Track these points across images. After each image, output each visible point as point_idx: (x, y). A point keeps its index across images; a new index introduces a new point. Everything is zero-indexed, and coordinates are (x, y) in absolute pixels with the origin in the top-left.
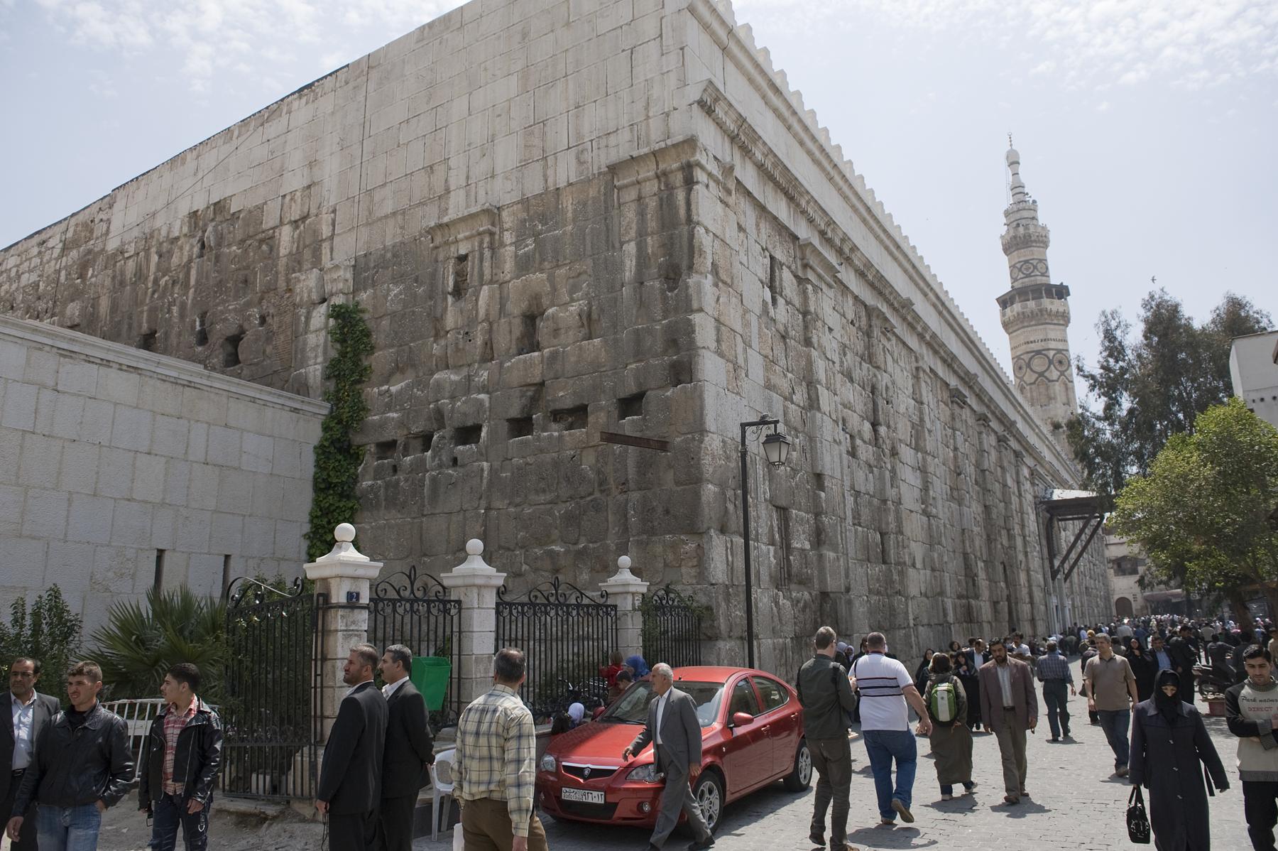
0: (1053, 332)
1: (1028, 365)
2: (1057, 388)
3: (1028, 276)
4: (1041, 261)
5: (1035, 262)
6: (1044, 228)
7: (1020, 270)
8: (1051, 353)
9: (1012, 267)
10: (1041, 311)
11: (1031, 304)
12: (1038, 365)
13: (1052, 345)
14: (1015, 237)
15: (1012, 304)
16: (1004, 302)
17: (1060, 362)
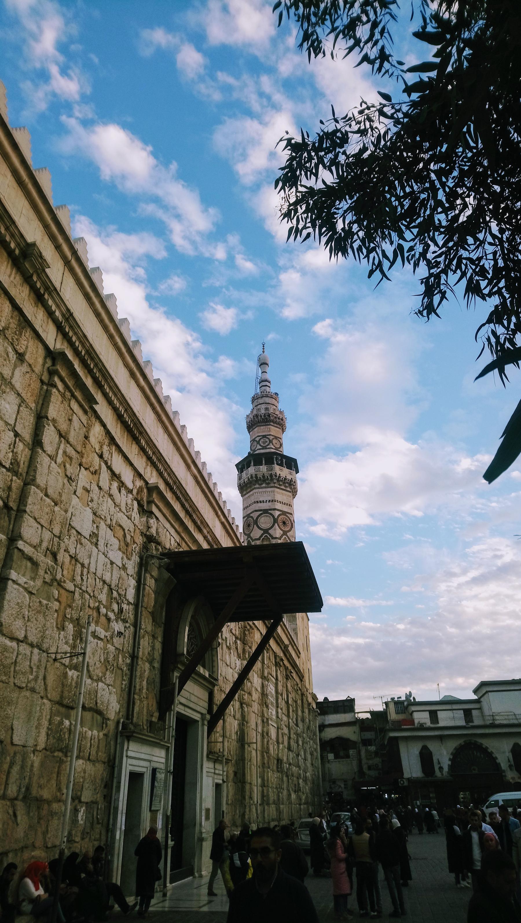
0: (280, 495)
1: (256, 522)
3: (264, 448)
4: (276, 438)
5: (271, 438)
6: (281, 412)
7: (258, 442)
8: (277, 513)
9: (253, 441)
11: (264, 468)
12: (265, 522)
13: (278, 506)
14: (257, 416)
15: (249, 466)
16: (241, 467)
17: (284, 523)
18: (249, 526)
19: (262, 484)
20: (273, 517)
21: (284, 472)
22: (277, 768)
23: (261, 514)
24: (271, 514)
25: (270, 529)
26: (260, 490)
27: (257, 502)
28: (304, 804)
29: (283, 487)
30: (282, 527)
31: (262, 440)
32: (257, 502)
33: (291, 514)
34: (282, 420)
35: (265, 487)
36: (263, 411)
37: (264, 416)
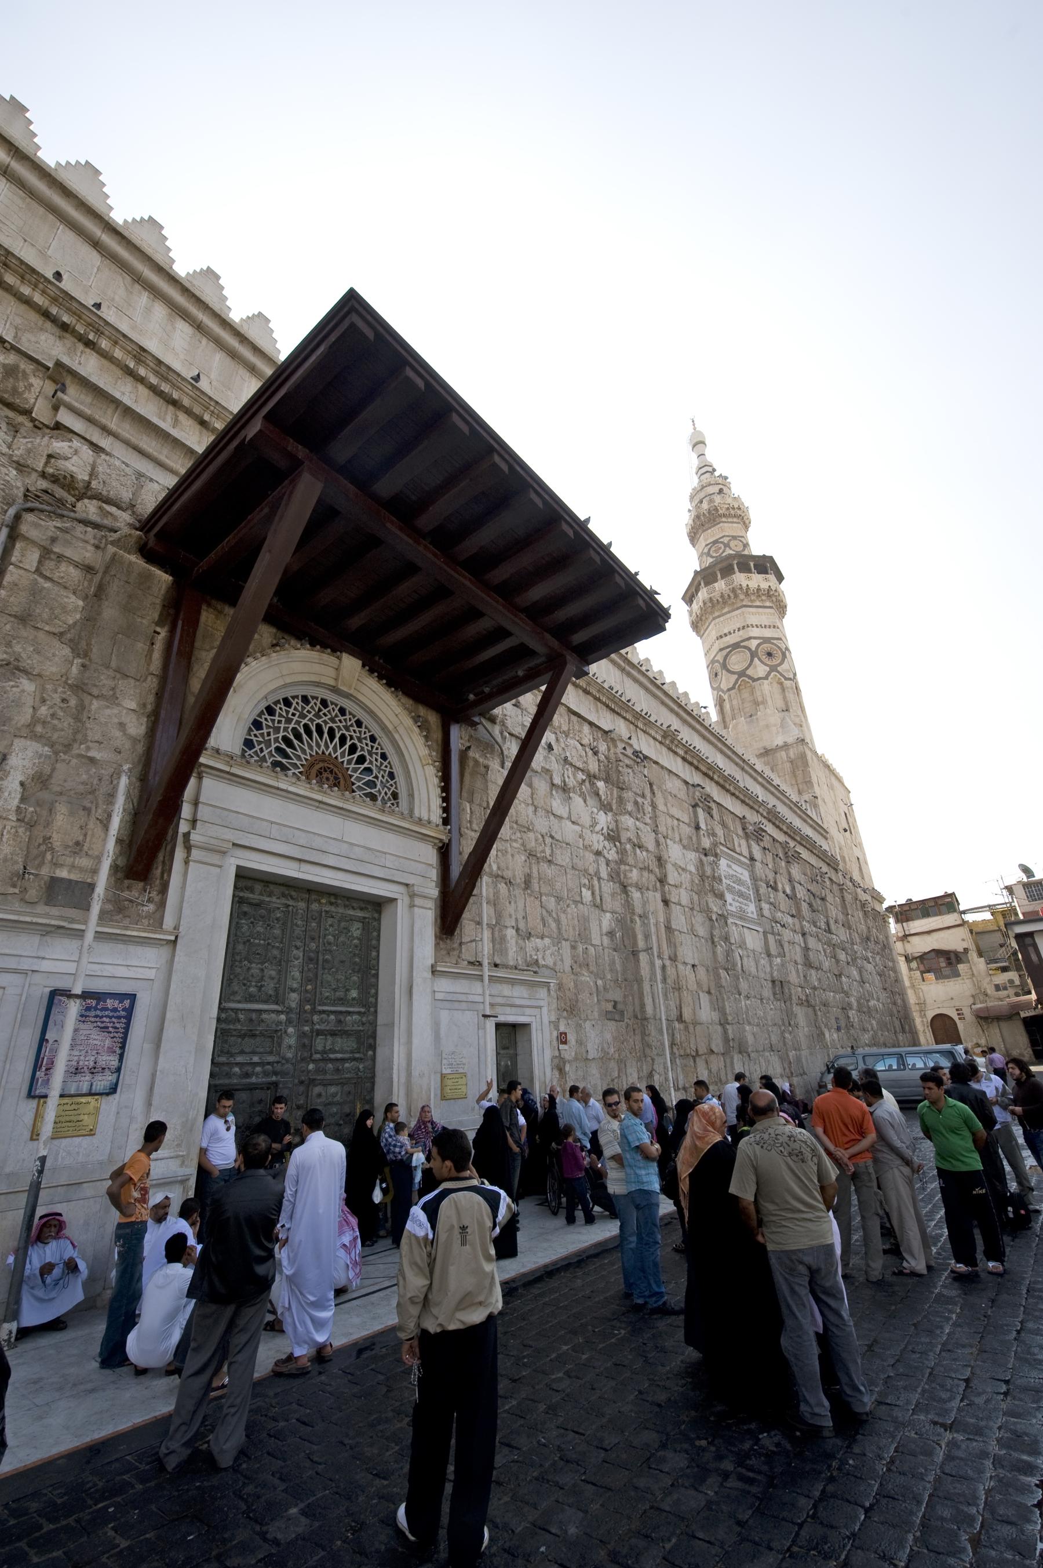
0: (757, 617)
1: (724, 666)
2: (767, 689)
5: (726, 540)
8: (753, 644)
10: (733, 590)
11: (721, 585)
12: (737, 661)
13: (755, 632)
17: (769, 654)
18: (716, 675)
19: (723, 608)
20: (749, 649)
21: (756, 581)
22: (775, 994)
23: (730, 652)
24: (745, 647)
25: (747, 668)
26: (722, 619)
27: (721, 637)
28: (867, 1045)
29: (758, 603)
30: (766, 661)
31: (713, 549)
32: (721, 637)
33: (780, 639)
34: (739, 509)
35: (729, 612)
36: (705, 506)
37: (709, 511)
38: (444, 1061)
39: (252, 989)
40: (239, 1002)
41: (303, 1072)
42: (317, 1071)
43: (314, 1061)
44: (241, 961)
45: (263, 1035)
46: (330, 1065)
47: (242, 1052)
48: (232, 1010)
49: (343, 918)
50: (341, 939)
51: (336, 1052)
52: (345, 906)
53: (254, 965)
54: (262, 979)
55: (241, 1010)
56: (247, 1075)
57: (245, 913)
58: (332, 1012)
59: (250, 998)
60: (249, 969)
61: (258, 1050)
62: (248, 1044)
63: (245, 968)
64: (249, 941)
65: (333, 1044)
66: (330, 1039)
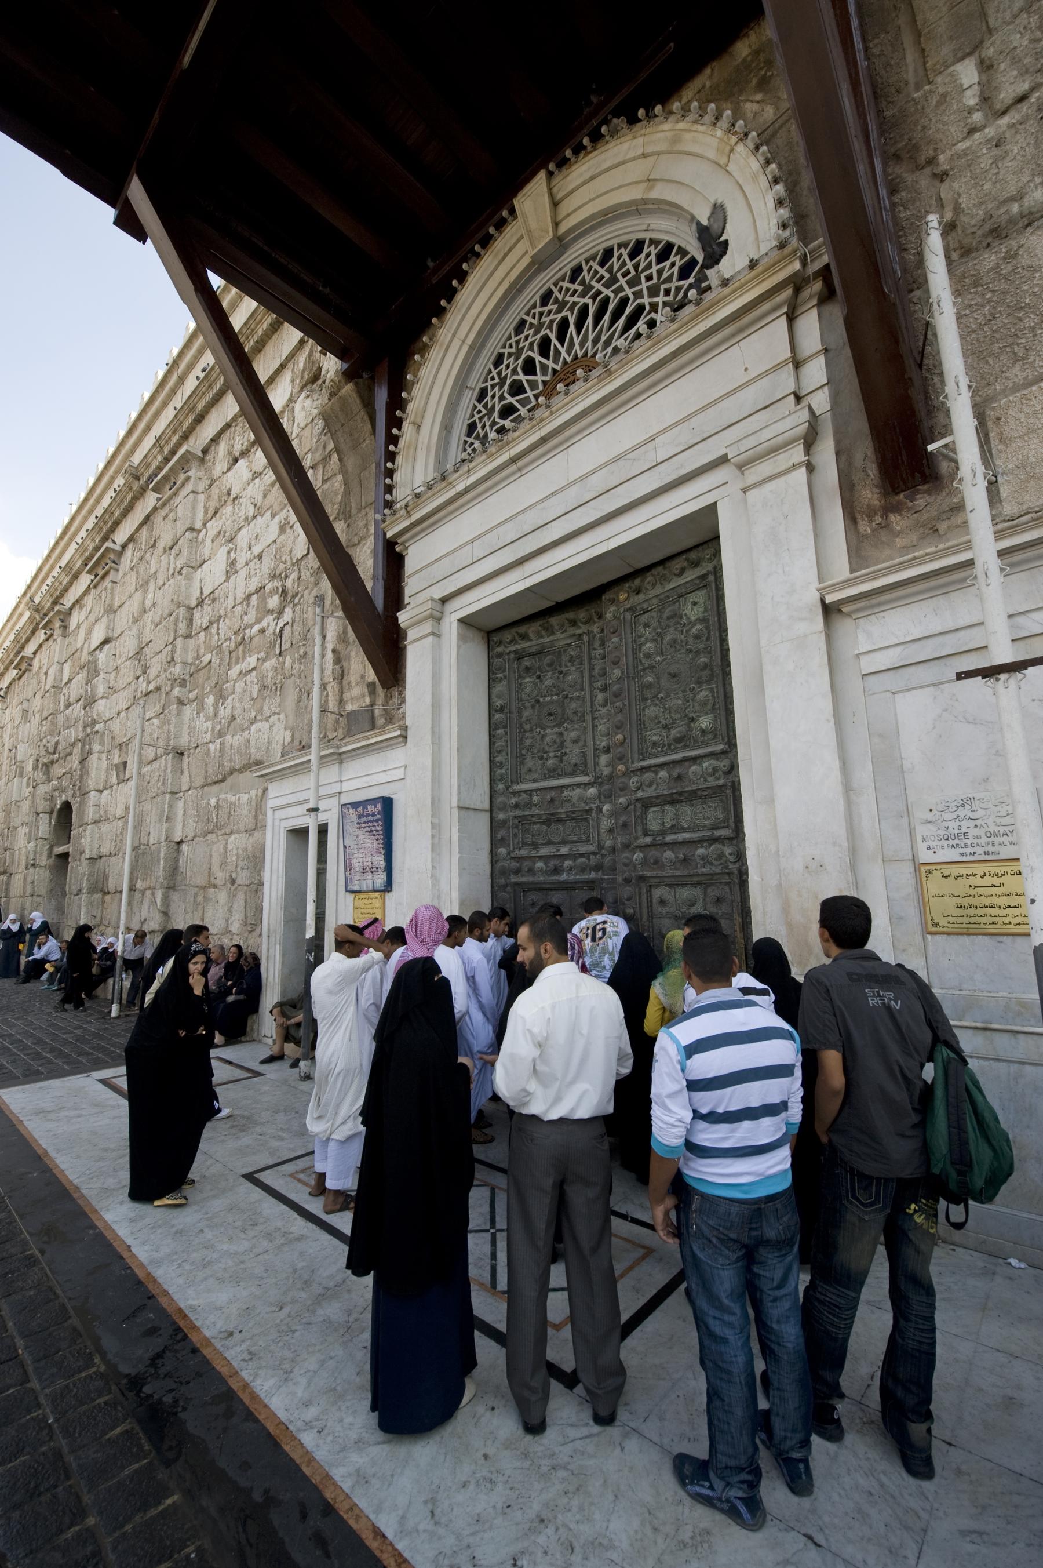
38: (921, 830)
39: (550, 762)
40: (535, 781)
41: (626, 865)
42: (645, 862)
43: (641, 848)
44: (531, 730)
45: (573, 819)
46: (669, 854)
47: (550, 843)
48: (525, 791)
49: (664, 602)
50: (668, 638)
51: (683, 830)
52: (664, 579)
53: (548, 731)
54: (562, 745)
55: (537, 790)
56: (556, 871)
57: (528, 669)
58: (662, 766)
59: (552, 773)
60: (543, 737)
61: (570, 838)
62: (557, 831)
63: (538, 738)
64: (538, 701)
65: (677, 817)
66: (670, 810)
